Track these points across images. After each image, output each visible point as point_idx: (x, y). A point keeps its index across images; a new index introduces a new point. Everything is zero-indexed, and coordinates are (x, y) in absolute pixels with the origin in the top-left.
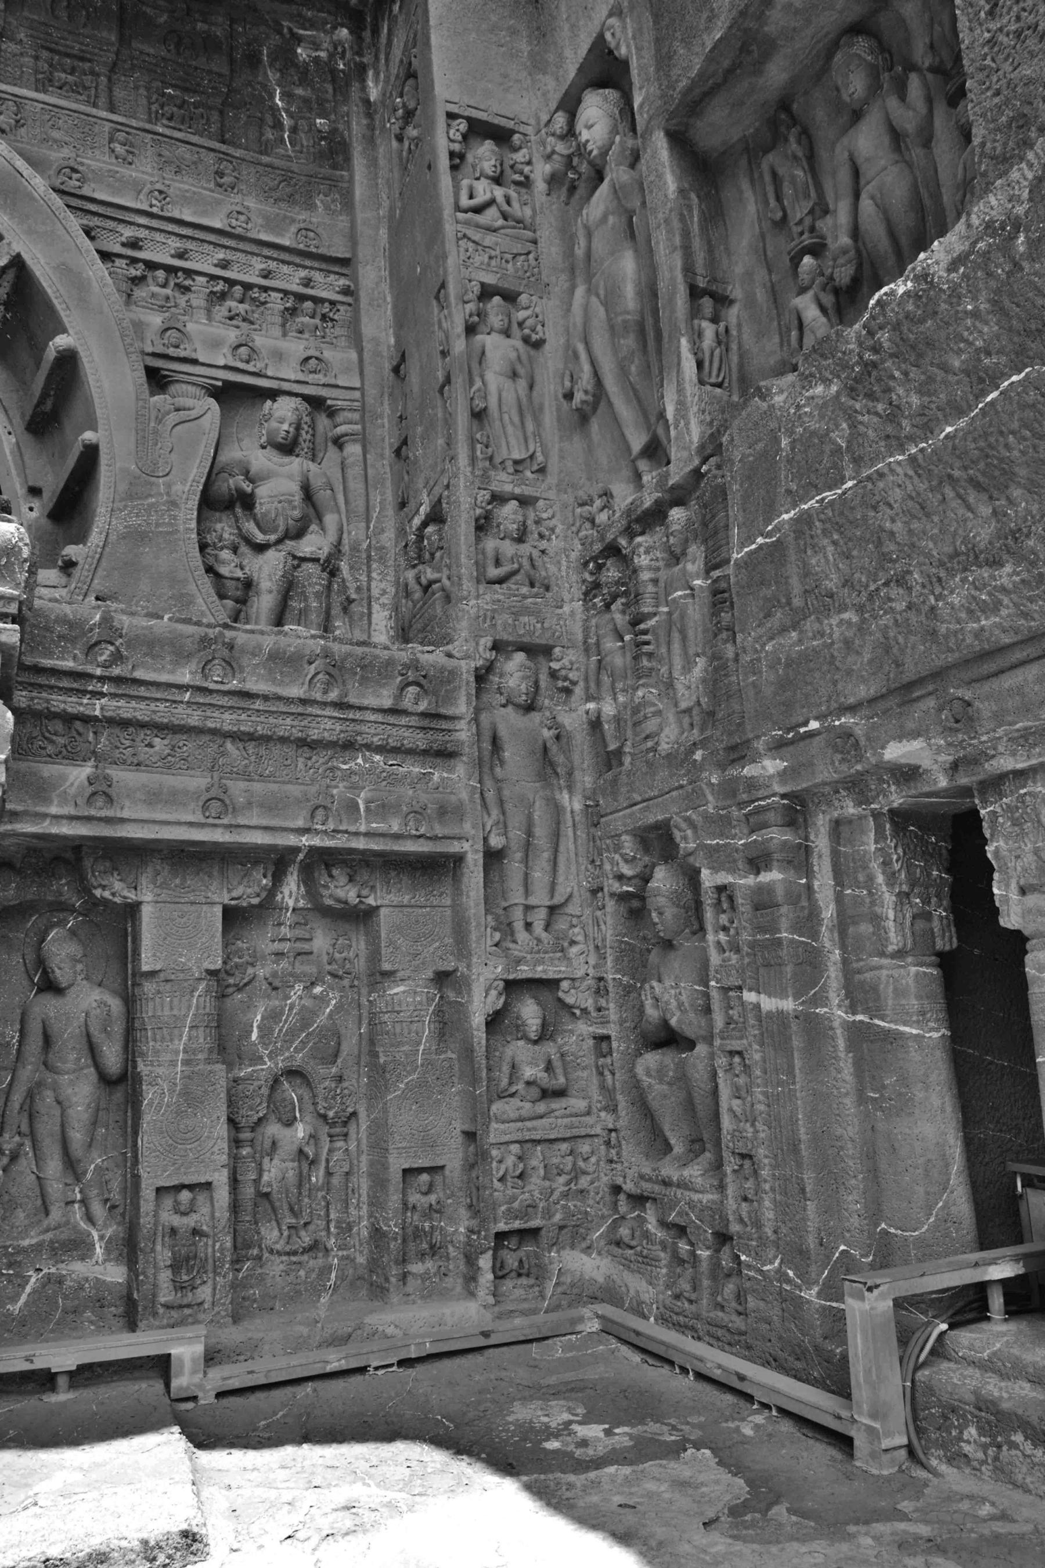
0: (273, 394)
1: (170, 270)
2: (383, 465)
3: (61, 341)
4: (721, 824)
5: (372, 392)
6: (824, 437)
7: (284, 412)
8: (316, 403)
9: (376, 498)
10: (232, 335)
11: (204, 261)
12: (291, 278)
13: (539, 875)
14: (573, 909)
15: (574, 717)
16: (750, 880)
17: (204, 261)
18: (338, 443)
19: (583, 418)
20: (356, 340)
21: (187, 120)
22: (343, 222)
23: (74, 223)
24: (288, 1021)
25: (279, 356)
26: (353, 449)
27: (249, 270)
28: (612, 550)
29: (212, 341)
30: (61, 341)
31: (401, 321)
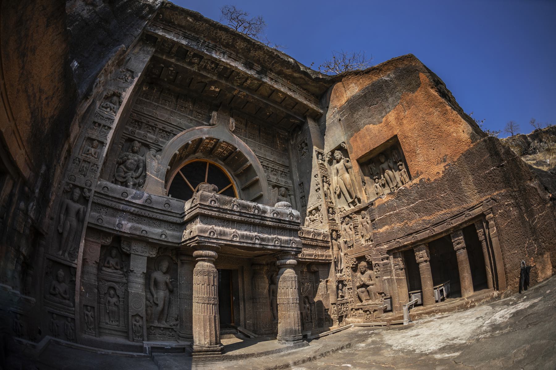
0: (281, 187)
1: (266, 166)
2: (298, 199)
3: (257, 177)
4: (377, 255)
5: (296, 188)
6: (393, 205)
7: (283, 189)
8: (287, 189)
9: (298, 205)
10: (275, 177)
11: (271, 165)
12: (282, 169)
13: (339, 265)
14: (344, 270)
15: (341, 240)
16: (382, 262)
17: (271, 165)
18: (290, 195)
19: (339, 196)
20: (291, 179)
21: (267, 144)
22: (288, 161)
23: (258, 159)
24: (305, 289)
25: (282, 181)
26: (292, 197)
27: (276, 167)
28: (348, 216)
29: (274, 179)
30: (257, 177)
31: (300, 177)
